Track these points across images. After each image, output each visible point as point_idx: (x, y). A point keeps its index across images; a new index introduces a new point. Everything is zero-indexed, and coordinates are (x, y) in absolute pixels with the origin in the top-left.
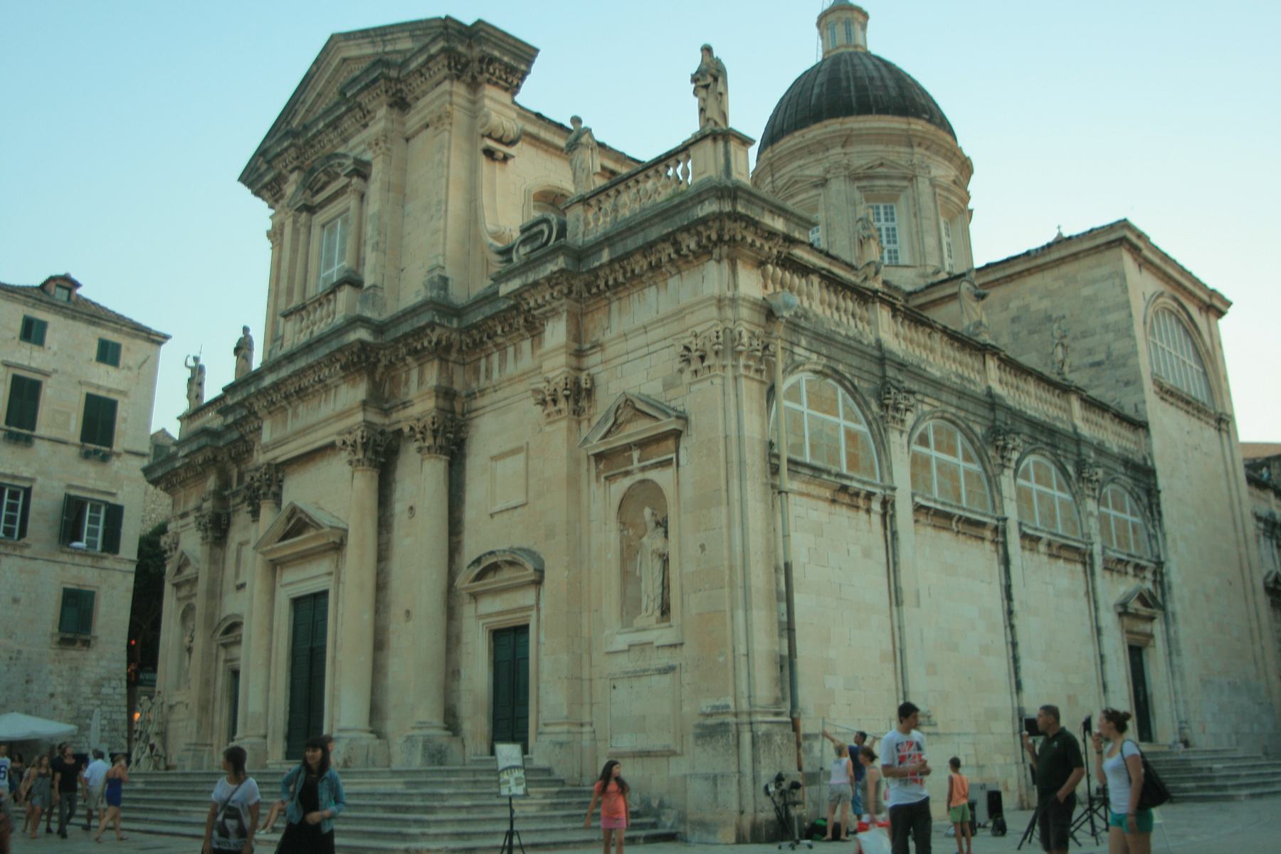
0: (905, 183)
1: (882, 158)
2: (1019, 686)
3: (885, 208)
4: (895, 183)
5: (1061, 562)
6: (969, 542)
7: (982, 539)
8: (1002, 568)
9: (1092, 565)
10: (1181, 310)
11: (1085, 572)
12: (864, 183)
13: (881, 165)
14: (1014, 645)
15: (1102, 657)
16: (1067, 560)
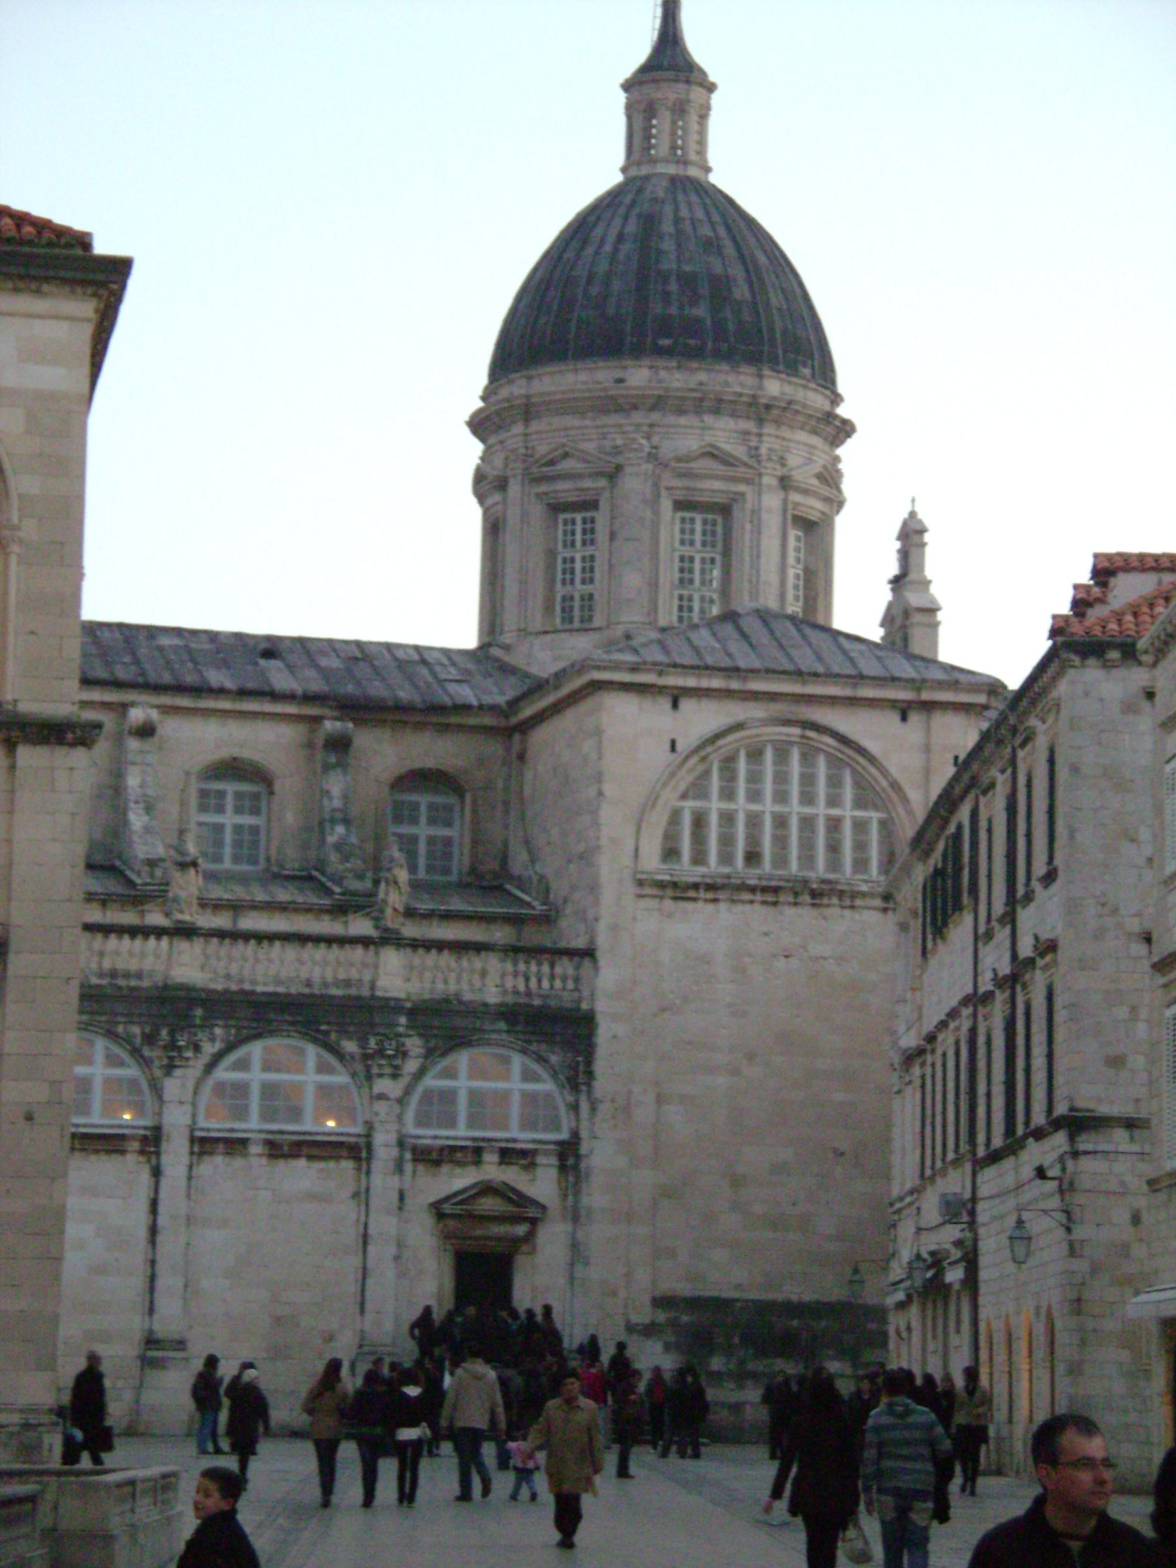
0: (602, 483)
1: (564, 445)
2: (151, 1310)
3: (584, 521)
4: (587, 483)
5: (302, 1162)
6: (93, 1157)
7: (123, 1152)
8: (153, 1180)
9: (369, 1159)
10: (811, 734)
11: (359, 1169)
12: (543, 488)
13: (566, 455)
14: (153, 1263)
15: (365, 1269)
16: (310, 1158)
